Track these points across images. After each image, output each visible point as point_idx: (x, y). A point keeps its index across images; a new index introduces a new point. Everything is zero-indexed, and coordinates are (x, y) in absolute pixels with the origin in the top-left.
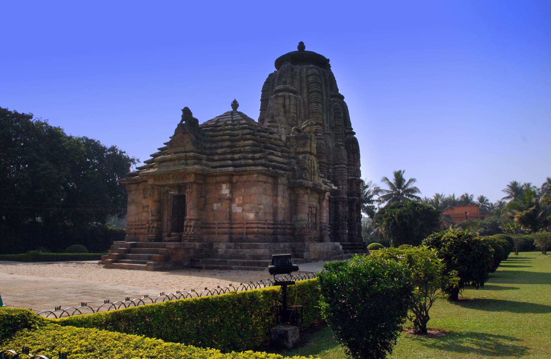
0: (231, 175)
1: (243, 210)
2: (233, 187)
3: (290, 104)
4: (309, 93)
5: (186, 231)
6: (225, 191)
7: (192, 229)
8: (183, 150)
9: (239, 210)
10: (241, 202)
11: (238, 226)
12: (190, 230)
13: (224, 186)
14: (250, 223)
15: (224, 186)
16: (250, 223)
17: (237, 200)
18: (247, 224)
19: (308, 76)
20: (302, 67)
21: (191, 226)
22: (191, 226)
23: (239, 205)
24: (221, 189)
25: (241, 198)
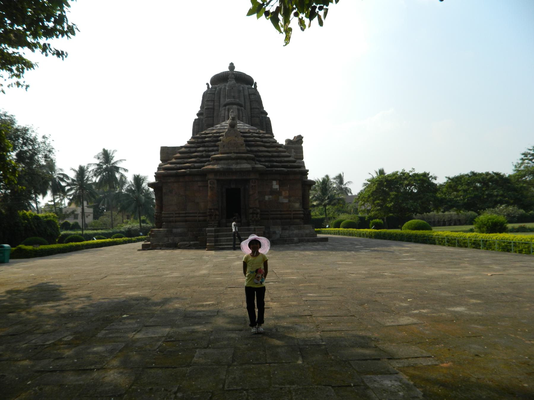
0: (280, 173)
1: (289, 201)
2: (281, 184)
3: (242, 116)
4: (251, 109)
5: (253, 217)
6: (276, 186)
7: (258, 215)
8: (237, 151)
9: (286, 201)
10: (287, 195)
11: (287, 212)
12: (257, 217)
13: (274, 183)
14: (296, 211)
15: (274, 183)
16: (296, 211)
17: (283, 193)
18: (294, 211)
19: (249, 95)
20: (242, 86)
21: (257, 214)
22: (257, 214)
23: (285, 197)
24: (272, 185)
25: (287, 192)
